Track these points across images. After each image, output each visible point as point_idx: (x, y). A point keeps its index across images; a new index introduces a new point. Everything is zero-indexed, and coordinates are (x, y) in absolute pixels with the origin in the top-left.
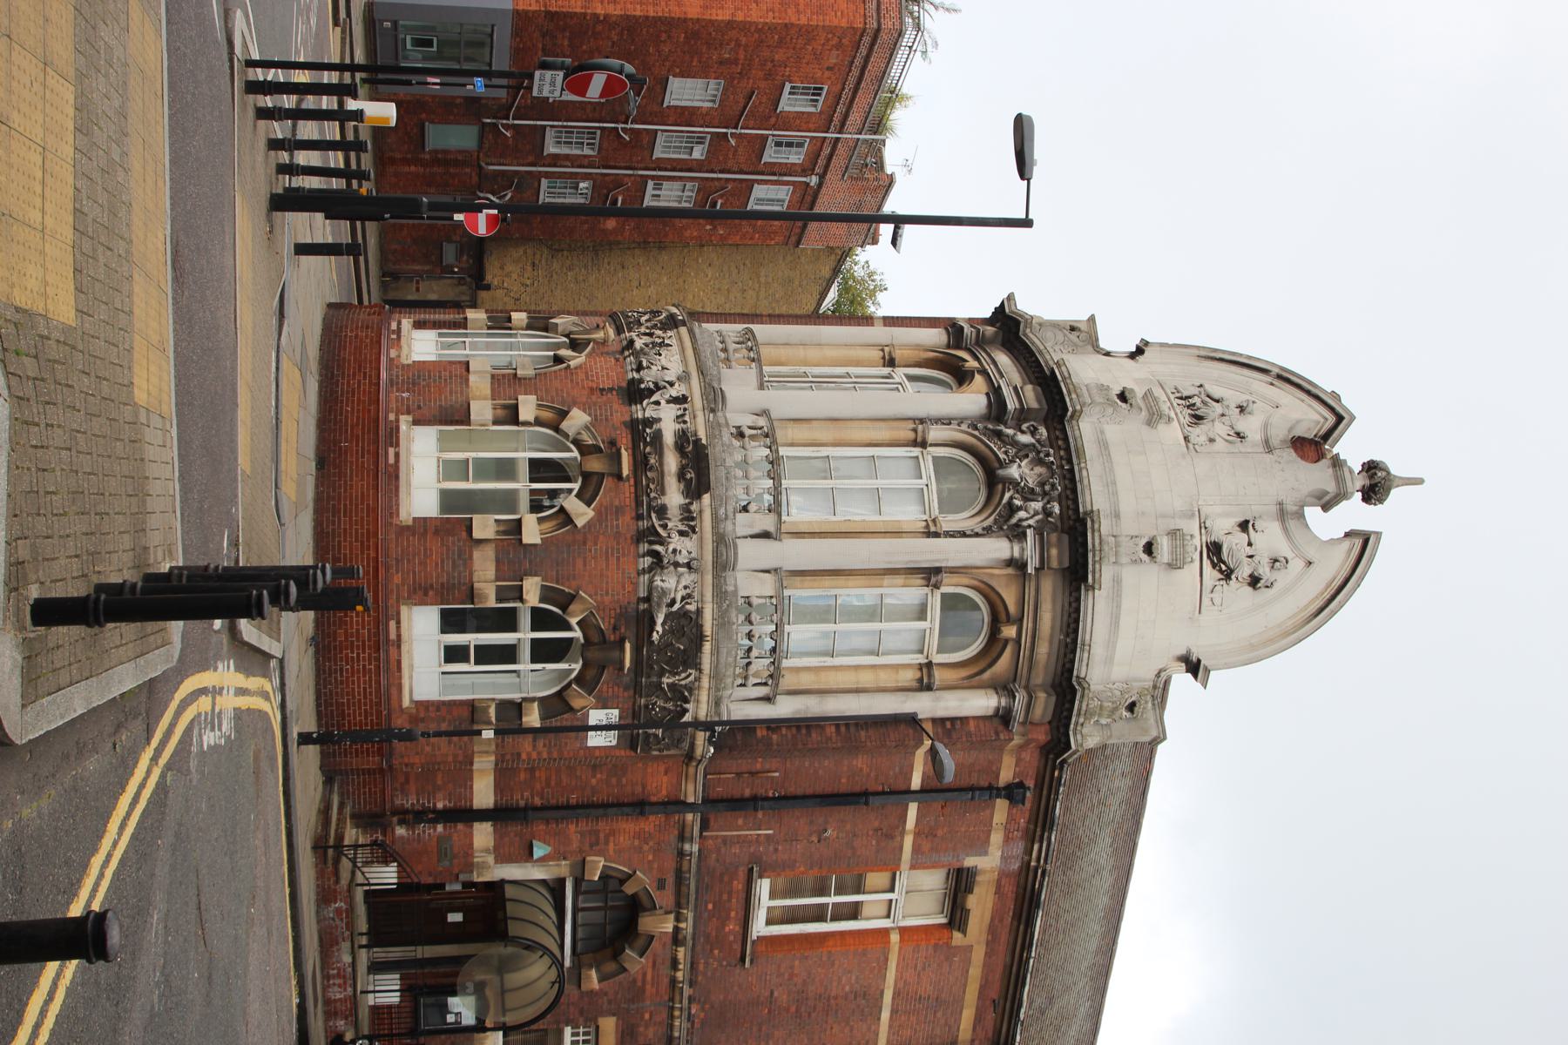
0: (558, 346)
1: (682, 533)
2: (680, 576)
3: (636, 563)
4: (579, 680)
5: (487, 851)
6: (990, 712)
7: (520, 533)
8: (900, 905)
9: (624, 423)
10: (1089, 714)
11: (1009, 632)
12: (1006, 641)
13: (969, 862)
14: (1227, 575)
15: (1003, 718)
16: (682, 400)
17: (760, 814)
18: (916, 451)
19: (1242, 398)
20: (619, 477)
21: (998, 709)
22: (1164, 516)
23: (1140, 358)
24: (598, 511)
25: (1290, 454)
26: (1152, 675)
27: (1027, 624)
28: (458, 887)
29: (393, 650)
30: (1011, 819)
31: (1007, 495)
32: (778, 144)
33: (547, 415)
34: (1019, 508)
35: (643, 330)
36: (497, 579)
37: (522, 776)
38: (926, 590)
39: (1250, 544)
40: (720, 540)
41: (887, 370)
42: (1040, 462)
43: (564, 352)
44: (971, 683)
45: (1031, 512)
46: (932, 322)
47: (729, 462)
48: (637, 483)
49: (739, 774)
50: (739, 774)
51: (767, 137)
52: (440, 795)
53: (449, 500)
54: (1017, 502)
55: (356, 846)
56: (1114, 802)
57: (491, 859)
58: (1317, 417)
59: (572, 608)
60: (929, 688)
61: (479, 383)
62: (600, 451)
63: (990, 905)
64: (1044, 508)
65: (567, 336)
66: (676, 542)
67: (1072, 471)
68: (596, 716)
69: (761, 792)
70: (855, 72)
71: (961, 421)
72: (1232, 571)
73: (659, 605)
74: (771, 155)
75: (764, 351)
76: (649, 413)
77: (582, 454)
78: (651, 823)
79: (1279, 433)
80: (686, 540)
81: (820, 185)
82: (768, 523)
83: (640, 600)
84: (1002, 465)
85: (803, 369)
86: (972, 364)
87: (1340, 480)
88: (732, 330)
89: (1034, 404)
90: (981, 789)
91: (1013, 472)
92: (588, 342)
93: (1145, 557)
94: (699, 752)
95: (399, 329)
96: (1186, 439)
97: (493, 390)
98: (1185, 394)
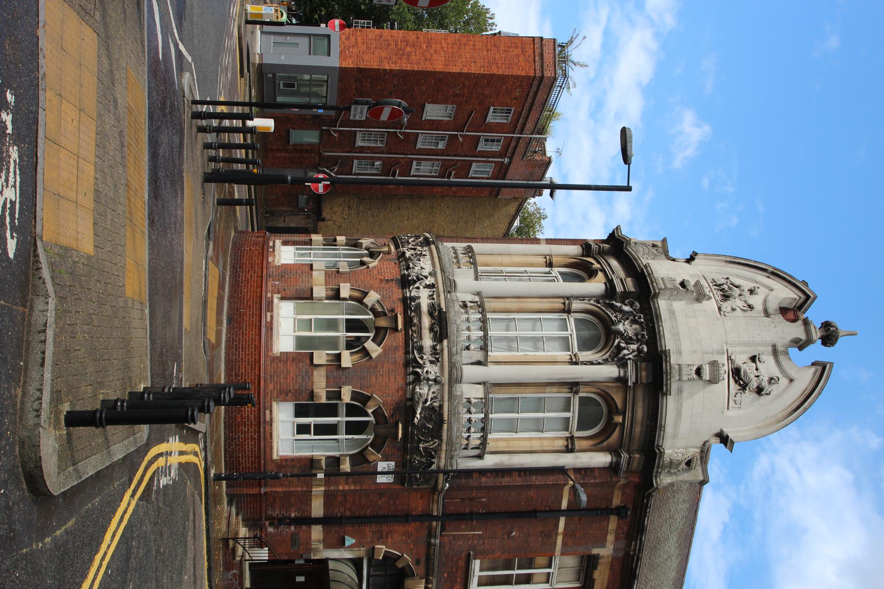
0: (362, 256)
1: (431, 362)
2: (430, 386)
3: (406, 379)
4: (372, 445)
5: (319, 541)
6: (607, 465)
7: (340, 361)
8: (555, 575)
9: (399, 299)
10: (663, 467)
11: (619, 419)
12: (616, 424)
13: (595, 551)
14: (744, 387)
15: (613, 468)
16: (432, 286)
17: (475, 523)
18: (565, 316)
19: (751, 285)
20: (395, 329)
21: (611, 463)
22: (707, 353)
23: (693, 263)
24: (384, 349)
25: (780, 317)
26: (700, 444)
27: (628, 415)
28: (302, 562)
29: (267, 427)
30: (619, 527)
31: (617, 341)
32: (486, 140)
33: (356, 294)
34: (624, 348)
35: (410, 246)
36: (327, 387)
37: (339, 499)
38: (570, 395)
39: (757, 369)
40: (452, 366)
41: (548, 269)
42: (634, 322)
43: (366, 259)
44: (596, 449)
45: (629, 351)
46: (573, 242)
47: (458, 322)
48: (407, 334)
49: (463, 500)
50: (463, 500)
51: (480, 136)
52: (293, 509)
53: (301, 342)
54: (623, 345)
55: (245, 538)
56: (678, 517)
57: (321, 546)
58: (795, 296)
59: (369, 404)
60: (572, 451)
61: (318, 277)
62: (385, 315)
63: (607, 577)
64: (638, 348)
65: (367, 249)
66: (429, 367)
68: (382, 466)
69: (475, 510)
70: (529, 100)
71: (590, 297)
72: (747, 385)
73: (418, 403)
74: (482, 147)
75: (479, 259)
77: (375, 316)
78: (412, 527)
79: (773, 306)
80: (434, 366)
81: (510, 163)
82: (478, 356)
83: (407, 400)
84: (613, 323)
85: (500, 268)
86: (596, 266)
87: (808, 332)
88: (460, 246)
89: (632, 289)
90: (602, 510)
91: (621, 327)
92: (380, 253)
93: (695, 376)
94: (440, 486)
95: (274, 246)
96: (720, 309)
97: (326, 280)
98: (719, 283)
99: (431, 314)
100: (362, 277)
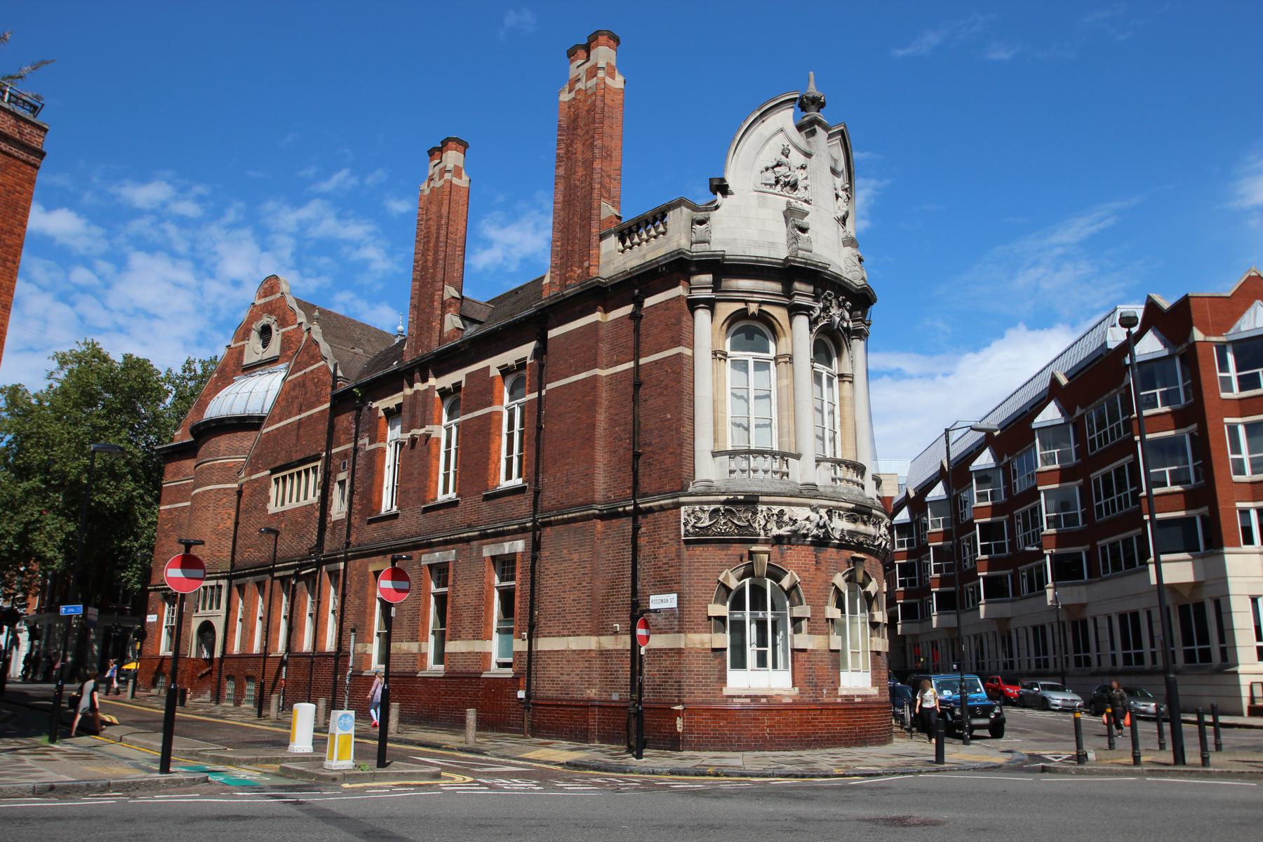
16: (830, 512)
58: (791, 112)
67: (840, 286)
76: (837, 535)
89: (811, 288)
99: (855, 521)
100: (813, 591)
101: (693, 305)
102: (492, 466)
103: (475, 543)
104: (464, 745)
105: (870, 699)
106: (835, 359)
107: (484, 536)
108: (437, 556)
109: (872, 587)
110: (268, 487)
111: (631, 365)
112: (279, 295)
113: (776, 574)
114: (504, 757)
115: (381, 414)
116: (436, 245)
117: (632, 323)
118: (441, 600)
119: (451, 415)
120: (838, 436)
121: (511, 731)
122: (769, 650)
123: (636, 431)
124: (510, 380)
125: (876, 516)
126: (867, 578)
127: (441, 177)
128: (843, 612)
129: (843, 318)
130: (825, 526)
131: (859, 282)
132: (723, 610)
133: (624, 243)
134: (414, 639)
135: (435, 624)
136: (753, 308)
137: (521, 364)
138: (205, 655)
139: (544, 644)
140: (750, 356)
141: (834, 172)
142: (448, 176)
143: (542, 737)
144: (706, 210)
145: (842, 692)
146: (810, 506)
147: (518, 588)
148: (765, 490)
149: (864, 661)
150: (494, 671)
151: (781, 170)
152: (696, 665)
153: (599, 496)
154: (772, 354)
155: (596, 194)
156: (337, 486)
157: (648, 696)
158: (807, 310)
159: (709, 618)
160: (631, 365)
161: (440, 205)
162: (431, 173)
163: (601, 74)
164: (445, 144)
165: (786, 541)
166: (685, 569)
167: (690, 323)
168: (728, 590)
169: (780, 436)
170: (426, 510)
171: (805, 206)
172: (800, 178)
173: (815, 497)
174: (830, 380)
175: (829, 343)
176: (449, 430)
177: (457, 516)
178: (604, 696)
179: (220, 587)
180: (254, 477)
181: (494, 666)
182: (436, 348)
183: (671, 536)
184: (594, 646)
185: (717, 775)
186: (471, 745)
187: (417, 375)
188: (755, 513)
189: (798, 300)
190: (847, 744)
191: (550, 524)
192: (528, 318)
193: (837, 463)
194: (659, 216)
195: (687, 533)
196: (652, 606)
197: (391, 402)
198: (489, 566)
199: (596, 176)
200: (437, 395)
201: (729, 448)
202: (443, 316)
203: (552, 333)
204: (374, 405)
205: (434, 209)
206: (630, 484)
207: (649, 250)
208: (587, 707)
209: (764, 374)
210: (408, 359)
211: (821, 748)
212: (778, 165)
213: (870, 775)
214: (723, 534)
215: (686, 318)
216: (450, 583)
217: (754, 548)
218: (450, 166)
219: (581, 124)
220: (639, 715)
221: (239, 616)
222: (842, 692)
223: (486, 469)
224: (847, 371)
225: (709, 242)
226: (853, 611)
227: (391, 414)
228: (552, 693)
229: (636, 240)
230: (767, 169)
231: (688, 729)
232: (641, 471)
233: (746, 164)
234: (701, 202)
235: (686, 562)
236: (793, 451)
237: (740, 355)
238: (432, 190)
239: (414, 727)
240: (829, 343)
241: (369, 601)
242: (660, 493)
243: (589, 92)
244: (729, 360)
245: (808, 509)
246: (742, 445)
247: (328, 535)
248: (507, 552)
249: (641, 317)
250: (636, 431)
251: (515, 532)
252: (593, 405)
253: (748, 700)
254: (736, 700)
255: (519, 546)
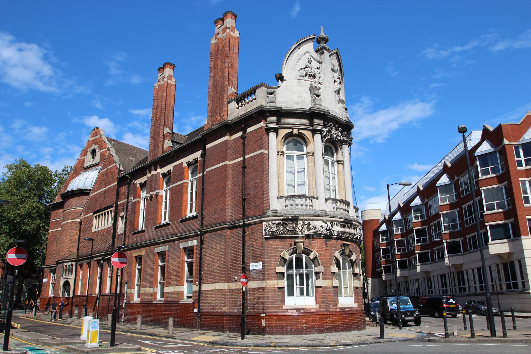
16: (332, 223)
67: (336, 120)
89: (322, 122)
99: (344, 227)
101: (268, 130)
102: (184, 207)
103: (176, 242)
104: (167, 335)
105: (353, 309)
106: (335, 154)
107: (180, 239)
108: (161, 249)
109: (353, 257)
110: (92, 220)
111: (241, 159)
112: (99, 136)
113: (307, 252)
114: (183, 340)
115: (138, 186)
116: (161, 110)
117: (242, 140)
118: (163, 268)
119: (167, 185)
120: (337, 188)
121: (192, 328)
122: (305, 287)
123: (244, 188)
124: (192, 168)
125: (355, 225)
126: (351, 253)
127: (163, 80)
128: (339, 269)
129: (338, 135)
130: (329, 229)
131: (345, 119)
132: (283, 269)
133: (238, 104)
134: (151, 286)
135: (161, 279)
136: (295, 131)
137: (196, 161)
138: (67, 296)
139: (205, 287)
140: (294, 153)
141: (333, 70)
142: (166, 79)
143: (204, 330)
144: (274, 88)
145: (339, 306)
146: (322, 220)
147: (195, 262)
148: (302, 213)
149: (351, 291)
150: (185, 300)
151: (308, 70)
152: (271, 295)
153: (228, 219)
154: (305, 152)
155: (226, 83)
156: (120, 219)
157: (249, 310)
158: (320, 132)
159: (277, 273)
160: (241, 159)
161: (162, 92)
162: (159, 78)
163: (228, 30)
164: (165, 65)
165: (311, 237)
166: (266, 251)
167: (266, 139)
168: (285, 260)
169: (309, 189)
170: (156, 228)
171: (319, 85)
172: (317, 73)
173: (325, 216)
174: (333, 163)
175: (331, 147)
176: (166, 192)
177: (169, 230)
178: (231, 310)
179: (72, 265)
180: (87, 216)
181: (185, 298)
182: (160, 155)
183: (259, 236)
184: (226, 288)
185: (275, 347)
186: (171, 334)
187: (153, 168)
188: (297, 224)
189: (316, 127)
190: (342, 330)
191: (207, 232)
192: (198, 140)
193: (336, 201)
194: (253, 91)
195: (266, 234)
196: (251, 268)
197: (142, 180)
198: (182, 252)
199: (226, 75)
200: (161, 176)
201: (286, 195)
202: (163, 141)
203: (208, 146)
204: (136, 182)
205: (160, 94)
206: (241, 213)
207: (249, 107)
208: (223, 315)
209: (301, 161)
210: (149, 161)
211: (330, 332)
212: (306, 67)
213: (347, 345)
214: (282, 234)
215: (265, 136)
216: (166, 260)
217: (297, 240)
218: (167, 75)
219: (220, 53)
220: (243, 318)
221: (81, 278)
222: (339, 306)
223: (181, 208)
224: (340, 159)
225: (275, 102)
226: (344, 268)
227: (143, 186)
228: (208, 310)
229: (244, 103)
230: (301, 69)
231: (268, 325)
232: (246, 206)
233: (291, 68)
234: (271, 85)
235: (266, 248)
236: (315, 196)
237: (290, 153)
238: (159, 86)
239: (150, 327)
240: (331, 147)
241: (133, 269)
242: (254, 216)
243: (223, 39)
244: (285, 155)
245: (322, 222)
246: (292, 193)
247: (116, 241)
248: (190, 246)
249: (246, 137)
250: (244, 188)
251: (193, 236)
252: (225, 178)
253: (295, 311)
254: (289, 311)
255: (195, 243)
